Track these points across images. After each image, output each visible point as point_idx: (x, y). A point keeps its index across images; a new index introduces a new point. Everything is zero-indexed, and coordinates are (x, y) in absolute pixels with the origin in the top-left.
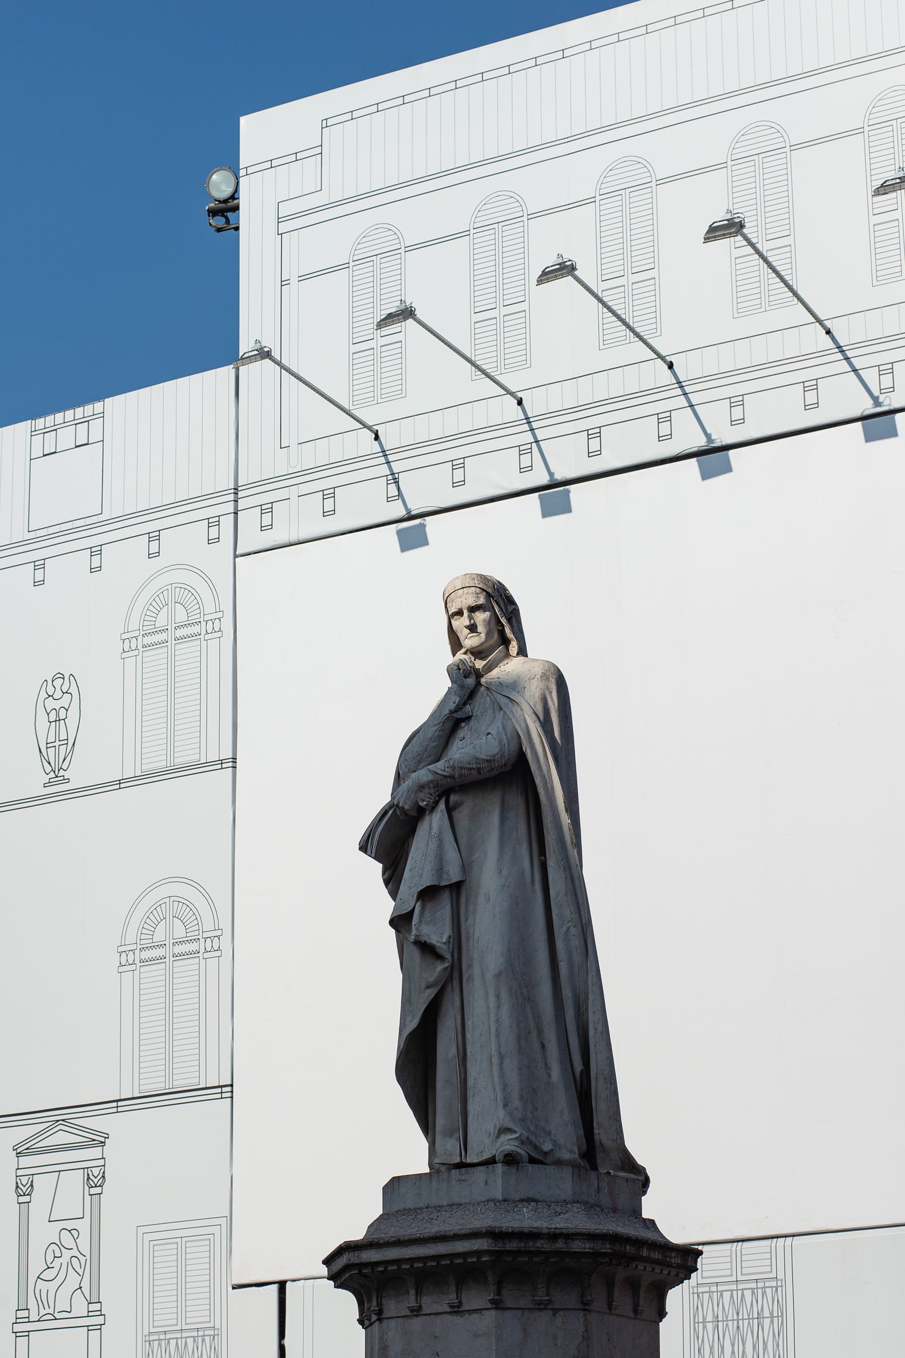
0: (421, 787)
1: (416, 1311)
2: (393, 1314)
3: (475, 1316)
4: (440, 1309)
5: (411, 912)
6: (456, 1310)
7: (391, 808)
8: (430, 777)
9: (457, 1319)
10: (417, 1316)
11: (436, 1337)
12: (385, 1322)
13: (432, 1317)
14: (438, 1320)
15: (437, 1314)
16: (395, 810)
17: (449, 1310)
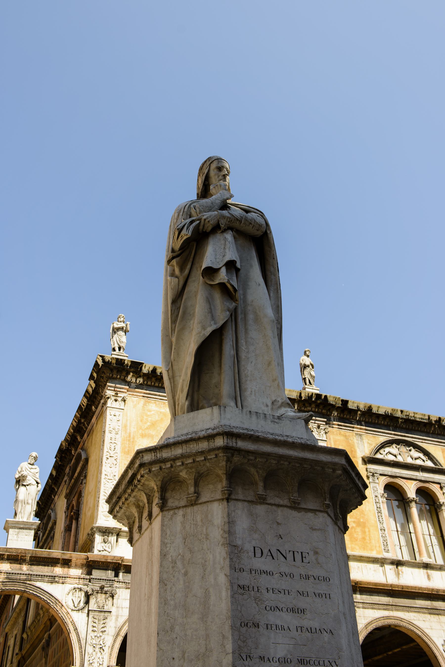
1: (261, 500)
2: (241, 497)
3: (310, 515)
4: (282, 503)
5: (217, 270)
6: (295, 506)
7: (198, 220)
8: (229, 215)
9: (294, 513)
10: (261, 503)
11: (278, 524)
12: (232, 503)
13: (274, 507)
14: (279, 511)
15: (279, 506)
16: (200, 222)
17: (289, 504)
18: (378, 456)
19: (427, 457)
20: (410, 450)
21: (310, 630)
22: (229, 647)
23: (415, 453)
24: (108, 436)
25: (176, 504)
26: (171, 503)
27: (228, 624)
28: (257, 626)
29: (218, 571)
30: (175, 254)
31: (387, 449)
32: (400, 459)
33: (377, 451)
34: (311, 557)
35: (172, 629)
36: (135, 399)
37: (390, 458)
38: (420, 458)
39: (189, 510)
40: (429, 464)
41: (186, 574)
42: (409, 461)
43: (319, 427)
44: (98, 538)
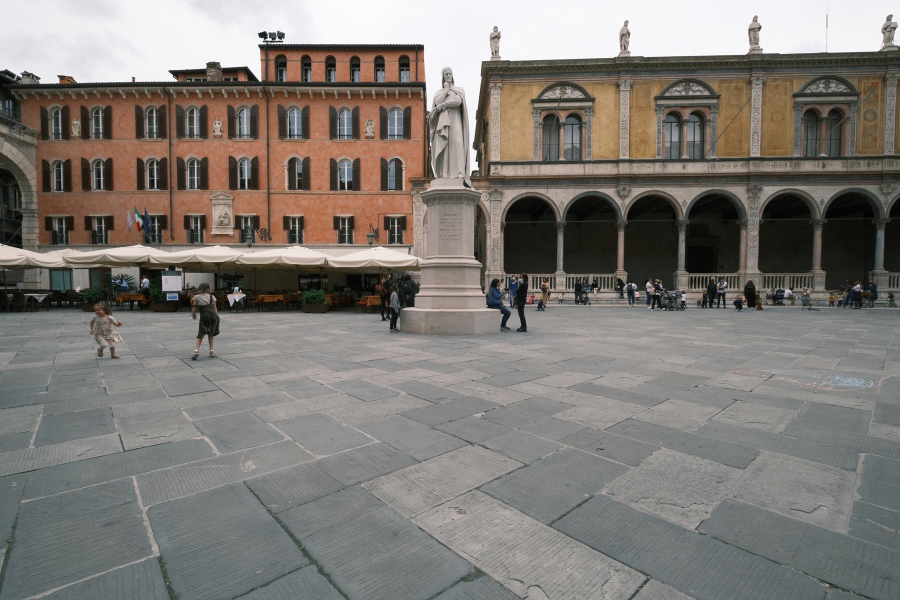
18: (667, 94)
23: (696, 88)
24: (493, 112)
31: (674, 89)
32: (684, 94)
33: (667, 90)
36: (507, 86)
37: (677, 94)
40: (706, 93)
42: (691, 93)
43: (625, 82)
44: (492, 168)
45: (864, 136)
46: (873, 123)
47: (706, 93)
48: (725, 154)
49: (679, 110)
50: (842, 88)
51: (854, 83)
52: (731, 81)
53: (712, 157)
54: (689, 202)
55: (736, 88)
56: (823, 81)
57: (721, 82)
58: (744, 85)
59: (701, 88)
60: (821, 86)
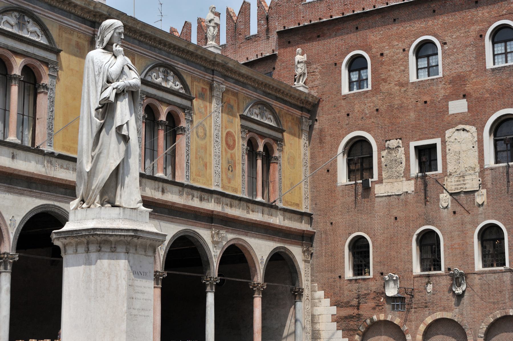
0: (127, 86)
9: (145, 257)
19: (43, 33)
20: (29, 22)
21: (146, 300)
22: (125, 305)
23: (32, 27)
25: (105, 250)
26: (103, 249)
27: (126, 297)
28: (133, 298)
29: (122, 279)
30: (100, 106)
31: (5, 18)
34: (148, 274)
35: (103, 297)
38: (36, 32)
39: (111, 254)
40: (43, 40)
41: (109, 278)
45: (196, 158)
46: (202, 142)
47: (43, 40)
48: (64, 148)
49: (9, 54)
50: (178, 86)
51: (188, 81)
52: (72, 31)
53: (50, 150)
54: (18, 220)
55: (77, 45)
56: (162, 69)
57: (61, 28)
58: (86, 44)
59: (37, 29)
60: (161, 76)
